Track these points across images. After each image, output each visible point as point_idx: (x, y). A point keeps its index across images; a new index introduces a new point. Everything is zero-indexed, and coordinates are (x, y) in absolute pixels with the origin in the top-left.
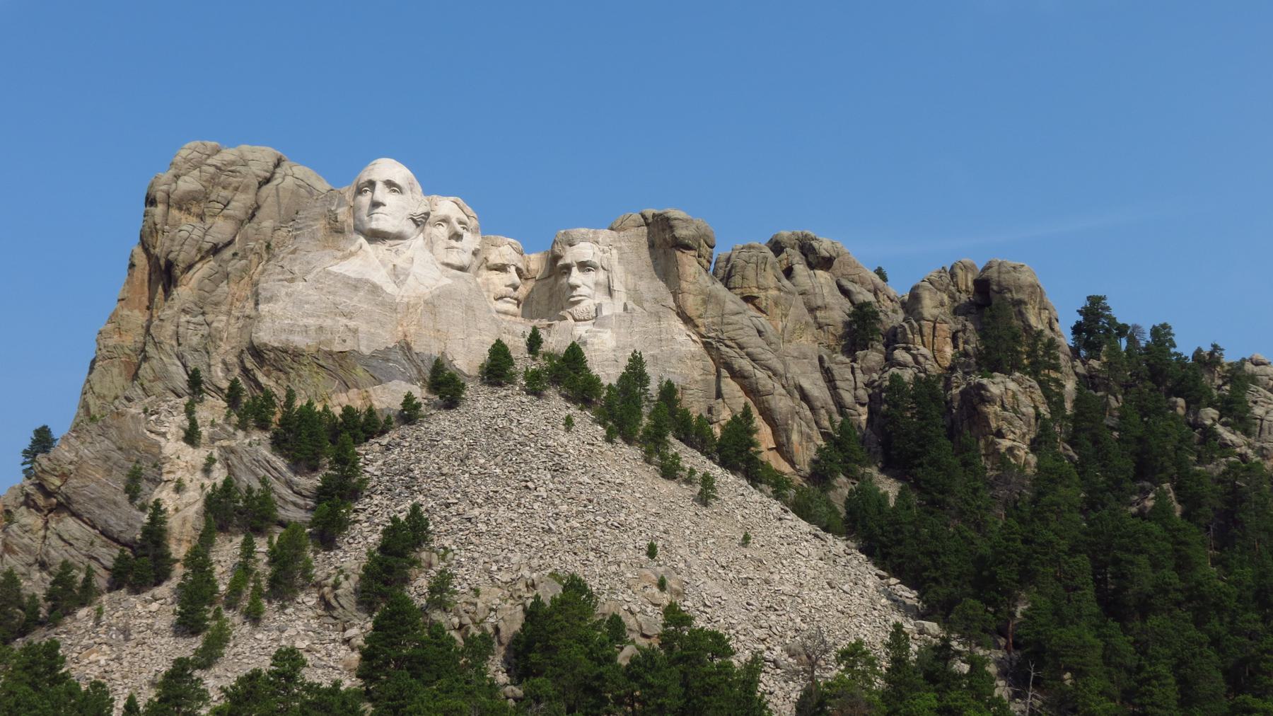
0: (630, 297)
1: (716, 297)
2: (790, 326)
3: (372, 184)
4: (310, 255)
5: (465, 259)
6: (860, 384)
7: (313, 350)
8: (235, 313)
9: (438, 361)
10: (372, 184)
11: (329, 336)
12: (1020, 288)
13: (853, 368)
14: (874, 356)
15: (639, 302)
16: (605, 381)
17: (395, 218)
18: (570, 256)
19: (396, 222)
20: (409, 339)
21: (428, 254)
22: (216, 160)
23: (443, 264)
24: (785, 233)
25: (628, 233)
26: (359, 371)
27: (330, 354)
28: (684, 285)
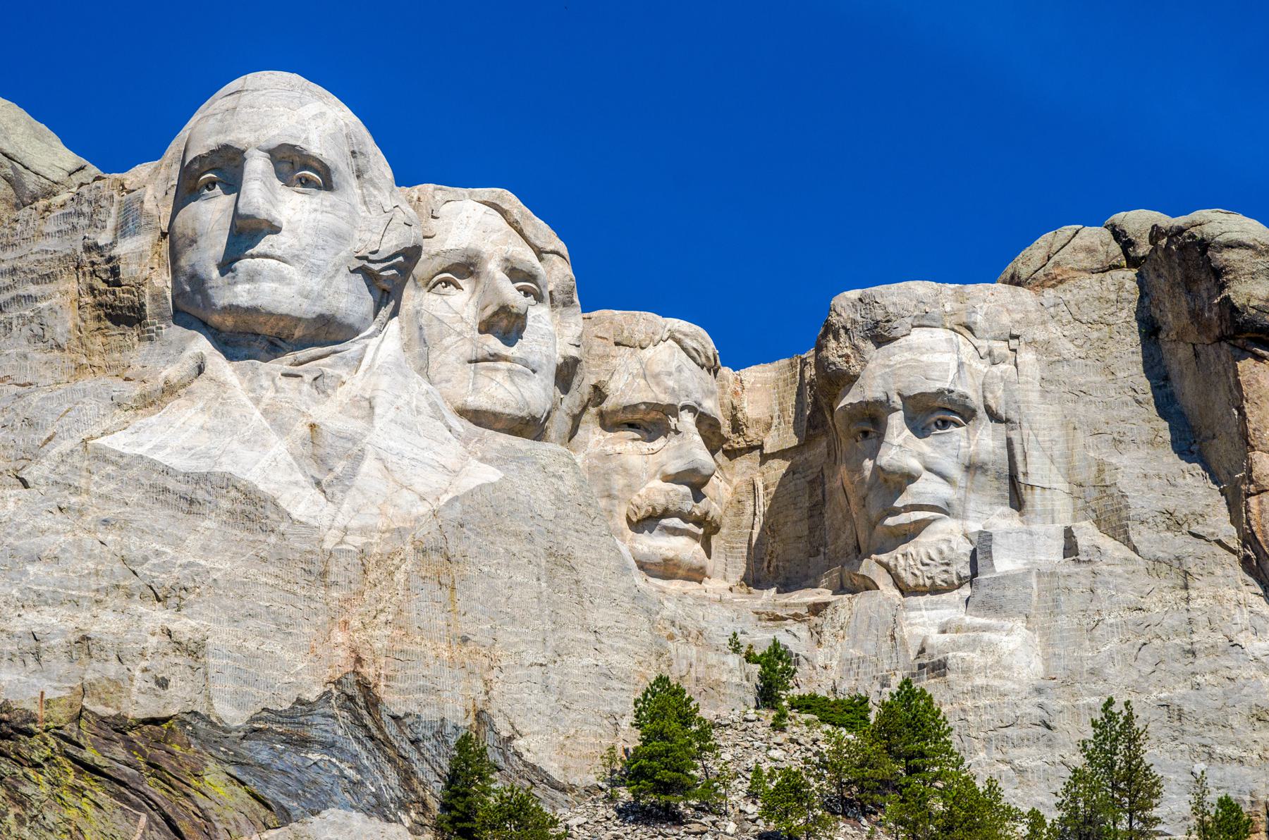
0: (1077, 514)
4: (36, 398)
5: (535, 393)
7: (60, 714)
9: (464, 743)
11: (113, 668)
15: (1116, 523)
16: (1012, 795)
17: (312, 271)
18: (879, 376)
19: (314, 284)
20: (369, 671)
21: (418, 385)
23: (463, 412)
25: (1068, 293)
27: (118, 727)
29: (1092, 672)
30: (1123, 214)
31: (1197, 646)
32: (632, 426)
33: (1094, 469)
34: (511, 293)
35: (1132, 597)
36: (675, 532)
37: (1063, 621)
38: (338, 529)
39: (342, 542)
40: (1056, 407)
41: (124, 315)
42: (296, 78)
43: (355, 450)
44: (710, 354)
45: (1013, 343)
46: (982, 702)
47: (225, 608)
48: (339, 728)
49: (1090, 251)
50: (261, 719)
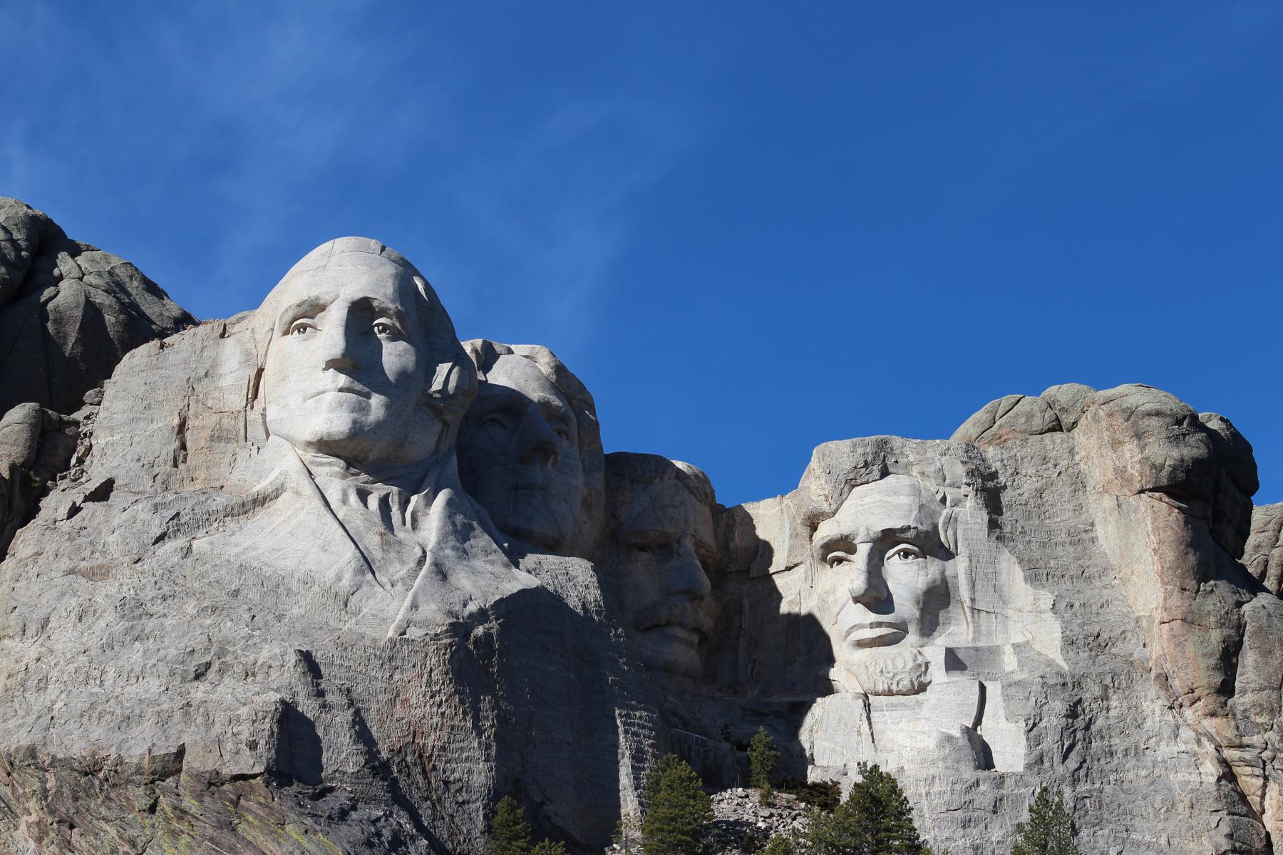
27: (213, 782)
29: (1029, 767)
30: (1057, 387)
31: (1114, 748)
32: (642, 549)
33: (1031, 597)
35: (1059, 705)
36: (674, 639)
37: (1003, 724)
38: (402, 621)
39: (404, 633)
40: (1001, 545)
42: (374, 244)
43: (419, 553)
44: (708, 491)
45: (964, 490)
46: (936, 788)
47: (306, 684)
49: (1030, 416)
50: (333, 779)
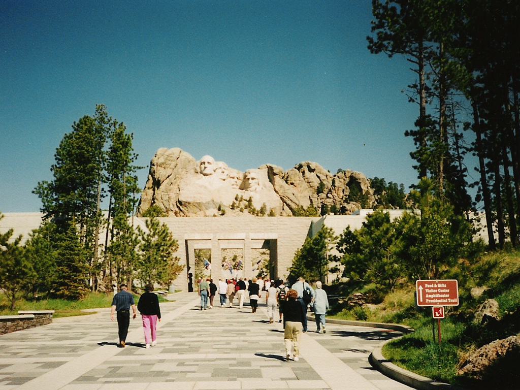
1: (283, 186)
2: (302, 189)
3: (204, 163)
6: (319, 203)
8: (174, 192)
10: (204, 163)
12: (360, 179)
13: (318, 199)
14: (323, 195)
15: (265, 187)
16: (257, 209)
22: (167, 153)
24: (303, 163)
26: (203, 207)
27: (197, 203)
28: (276, 183)
34: (224, 170)
41: (197, 173)
48: (211, 202)
